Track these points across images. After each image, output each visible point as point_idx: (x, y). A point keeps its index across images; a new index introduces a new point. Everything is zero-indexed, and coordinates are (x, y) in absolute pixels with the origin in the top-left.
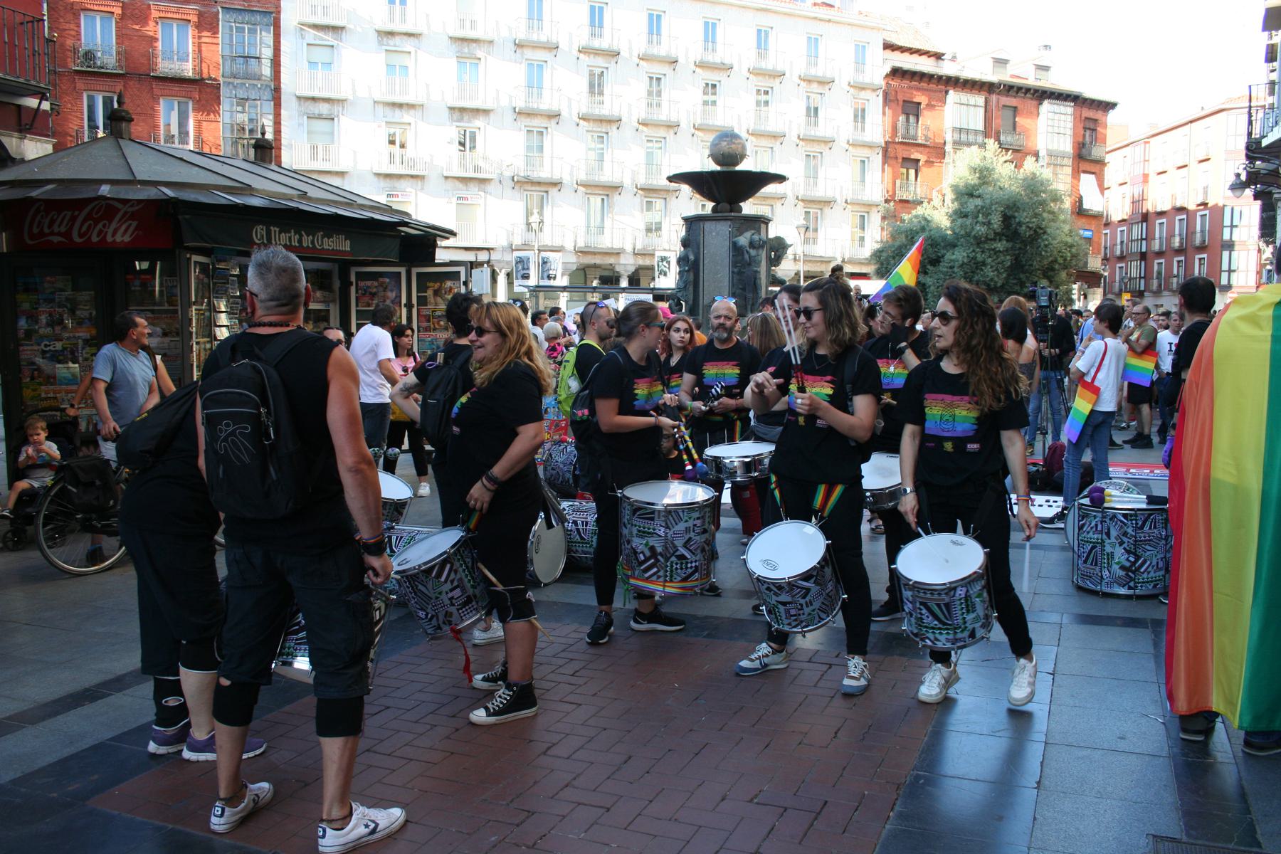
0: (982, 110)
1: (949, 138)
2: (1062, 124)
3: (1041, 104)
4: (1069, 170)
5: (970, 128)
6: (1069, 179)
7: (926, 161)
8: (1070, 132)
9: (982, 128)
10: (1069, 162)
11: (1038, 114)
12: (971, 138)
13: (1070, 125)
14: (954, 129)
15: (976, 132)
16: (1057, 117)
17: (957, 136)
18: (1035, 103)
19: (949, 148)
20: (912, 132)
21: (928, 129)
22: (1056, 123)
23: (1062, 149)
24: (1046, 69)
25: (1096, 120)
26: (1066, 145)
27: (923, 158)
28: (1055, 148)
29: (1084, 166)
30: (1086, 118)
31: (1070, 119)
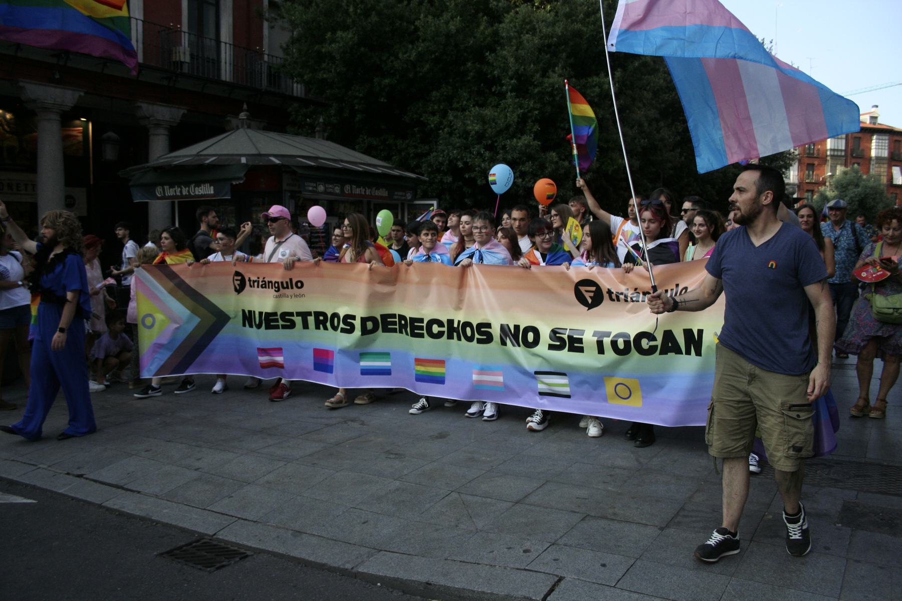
0: (844, 141)
1: (828, 153)
2: (883, 144)
3: (873, 135)
4: (886, 166)
5: (840, 148)
6: (886, 170)
7: (818, 165)
8: (887, 148)
9: (843, 148)
10: (886, 162)
11: (871, 140)
12: (839, 153)
13: (887, 145)
14: (831, 150)
15: (841, 150)
16: (881, 141)
17: (832, 153)
18: (869, 134)
19: (829, 158)
20: (812, 152)
21: (819, 150)
22: (880, 144)
23: (883, 156)
24: (876, 118)
25: (900, 141)
26: (885, 154)
27: (816, 163)
28: (880, 155)
29: (894, 163)
30: (896, 141)
31: (887, 141)
